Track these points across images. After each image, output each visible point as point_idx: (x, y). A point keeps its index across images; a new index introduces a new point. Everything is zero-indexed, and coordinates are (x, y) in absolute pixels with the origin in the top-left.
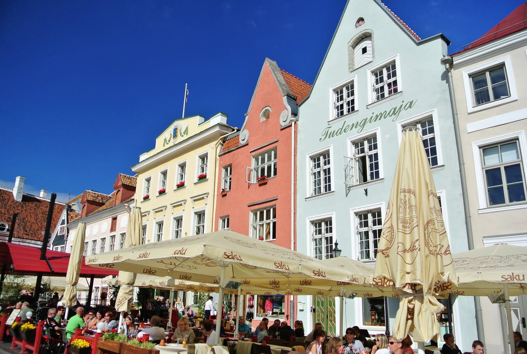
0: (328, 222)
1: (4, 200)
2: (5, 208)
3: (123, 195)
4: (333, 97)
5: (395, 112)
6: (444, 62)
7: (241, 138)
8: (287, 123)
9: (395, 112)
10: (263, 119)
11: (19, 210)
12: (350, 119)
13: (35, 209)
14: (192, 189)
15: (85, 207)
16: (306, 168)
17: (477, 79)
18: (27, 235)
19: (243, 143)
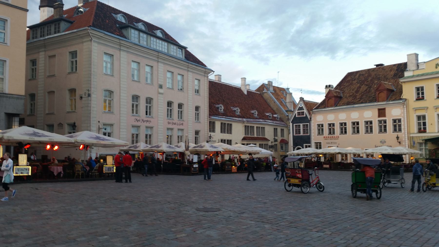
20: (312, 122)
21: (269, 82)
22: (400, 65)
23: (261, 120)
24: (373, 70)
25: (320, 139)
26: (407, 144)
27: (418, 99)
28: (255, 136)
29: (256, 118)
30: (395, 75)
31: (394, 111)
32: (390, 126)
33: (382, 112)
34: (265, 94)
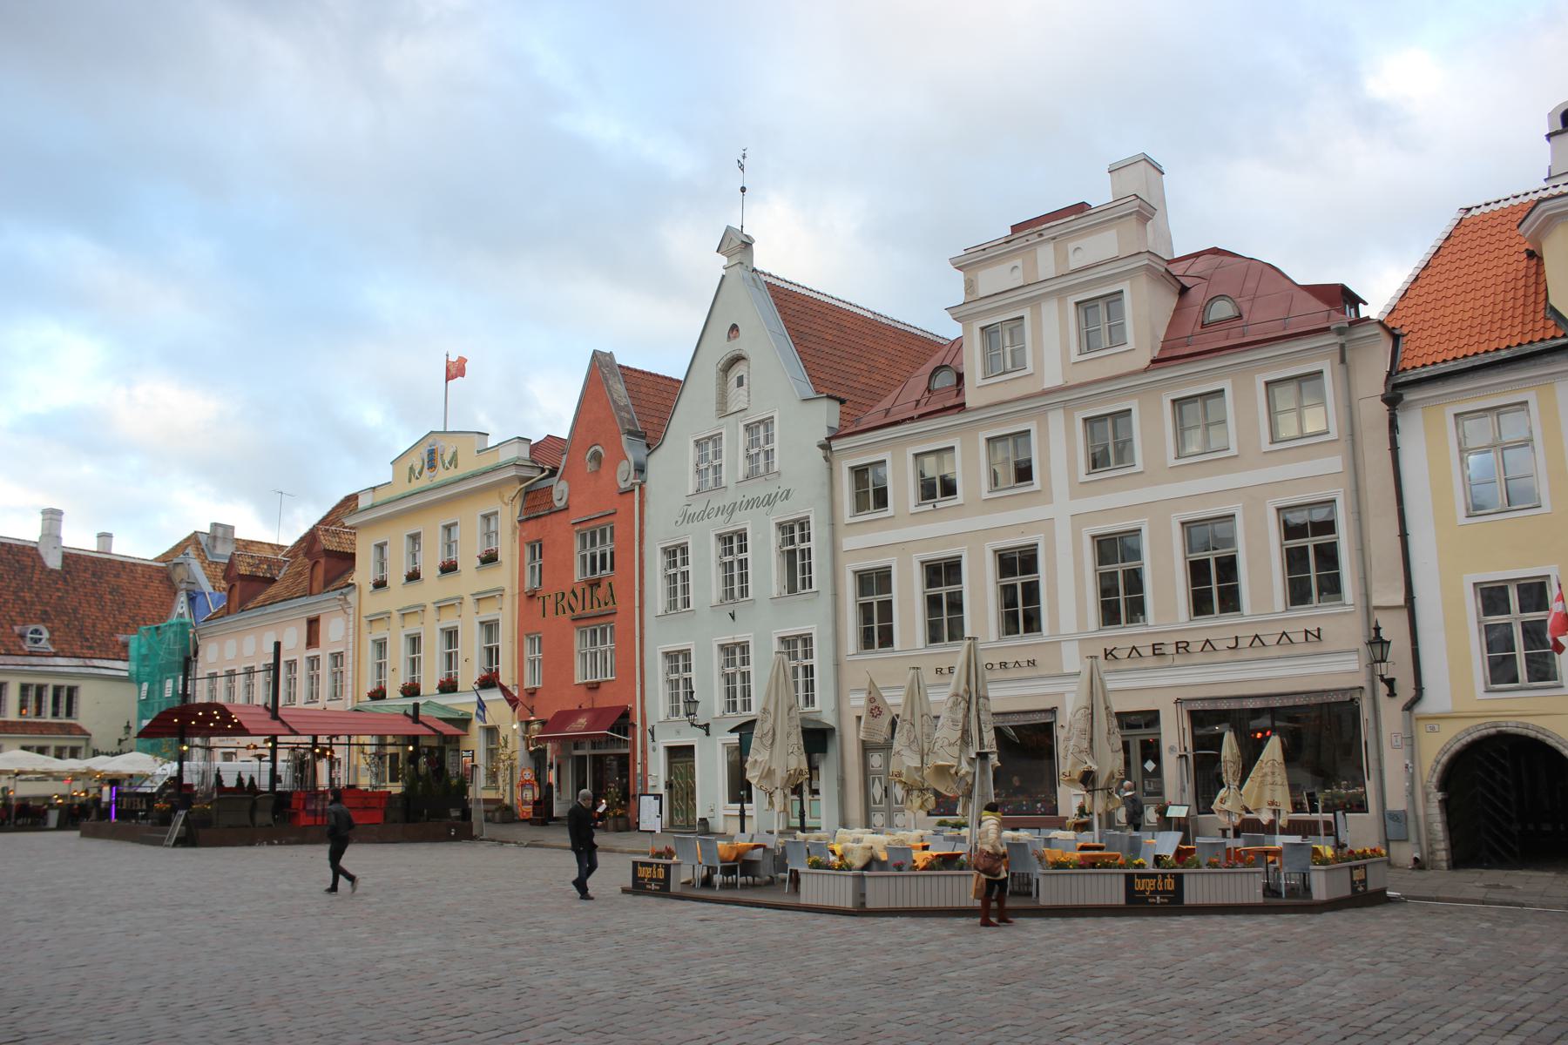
1: (23, 569)
2: (30, 589)
3: (327, 572)
4: (692, 453)
5: (769, 501)
6: (822, 446)
7: (556, 496)
8: (628, 485)
9: (769, 501)
10: (590, 467)
11: (58, 590)
12: (719, 500)
13: (94, 584)
14: (470, 579)
15: (237, 591)
16: (656, 565)
17: (860, 473)
18: (90, 648)
19: (559, 505)
21: (215, 526)
23: (60, 661)
28: (48, 717)
29: (31, 654)
34: (179, 570)
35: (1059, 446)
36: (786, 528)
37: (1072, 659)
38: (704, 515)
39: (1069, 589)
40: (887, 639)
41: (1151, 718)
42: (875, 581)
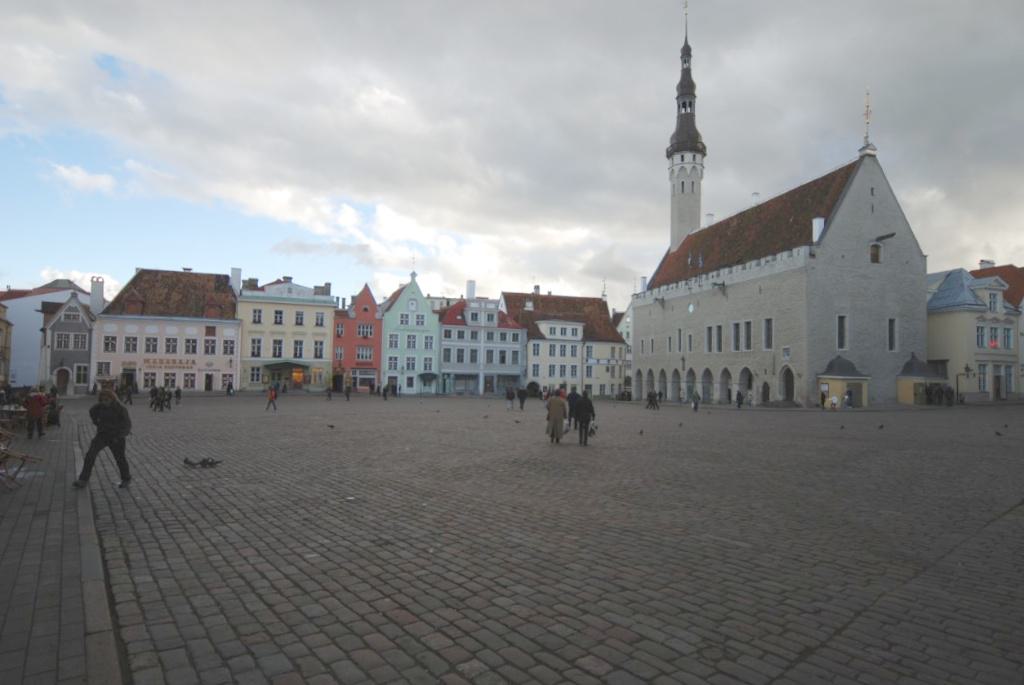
0: (396, 359)
9: (423, 331)
17: (446, 331)
20: (94, 333)
22: (218, 277)
24: (181, 274)
25: (106, 357)
26: (239, 369)
27: (255, 322)
30: (217, 289)
31: (226, 331)
32: (220, 347)
33: (211, 331)
35: (482, 335)
36: (427, 338)
37: (482, 367)
38: (403, 330)
39: (482, 357)
40: (449, 361)
41: (492, 377)
42: (447, 351)
